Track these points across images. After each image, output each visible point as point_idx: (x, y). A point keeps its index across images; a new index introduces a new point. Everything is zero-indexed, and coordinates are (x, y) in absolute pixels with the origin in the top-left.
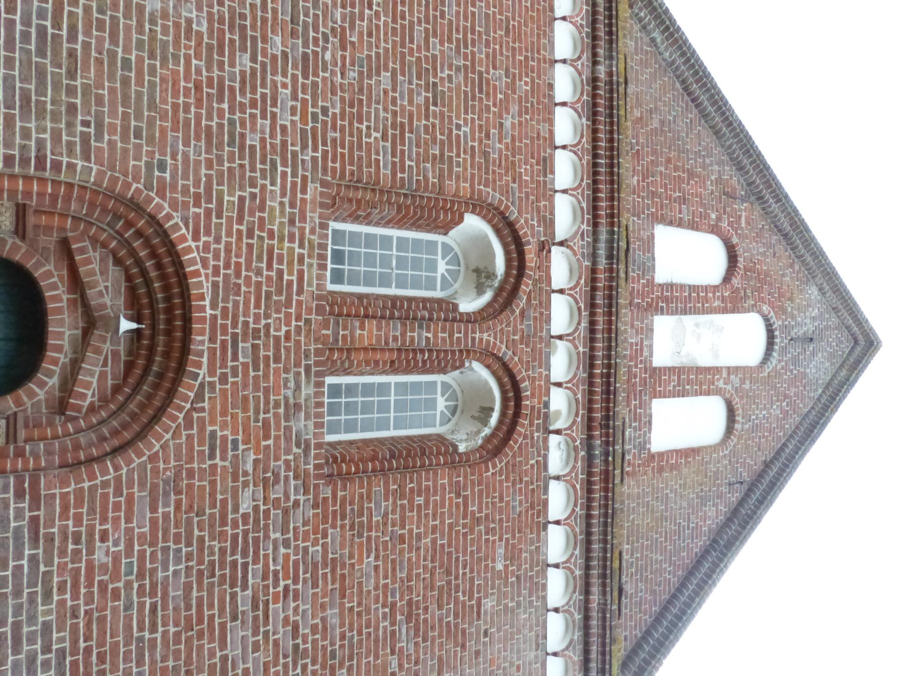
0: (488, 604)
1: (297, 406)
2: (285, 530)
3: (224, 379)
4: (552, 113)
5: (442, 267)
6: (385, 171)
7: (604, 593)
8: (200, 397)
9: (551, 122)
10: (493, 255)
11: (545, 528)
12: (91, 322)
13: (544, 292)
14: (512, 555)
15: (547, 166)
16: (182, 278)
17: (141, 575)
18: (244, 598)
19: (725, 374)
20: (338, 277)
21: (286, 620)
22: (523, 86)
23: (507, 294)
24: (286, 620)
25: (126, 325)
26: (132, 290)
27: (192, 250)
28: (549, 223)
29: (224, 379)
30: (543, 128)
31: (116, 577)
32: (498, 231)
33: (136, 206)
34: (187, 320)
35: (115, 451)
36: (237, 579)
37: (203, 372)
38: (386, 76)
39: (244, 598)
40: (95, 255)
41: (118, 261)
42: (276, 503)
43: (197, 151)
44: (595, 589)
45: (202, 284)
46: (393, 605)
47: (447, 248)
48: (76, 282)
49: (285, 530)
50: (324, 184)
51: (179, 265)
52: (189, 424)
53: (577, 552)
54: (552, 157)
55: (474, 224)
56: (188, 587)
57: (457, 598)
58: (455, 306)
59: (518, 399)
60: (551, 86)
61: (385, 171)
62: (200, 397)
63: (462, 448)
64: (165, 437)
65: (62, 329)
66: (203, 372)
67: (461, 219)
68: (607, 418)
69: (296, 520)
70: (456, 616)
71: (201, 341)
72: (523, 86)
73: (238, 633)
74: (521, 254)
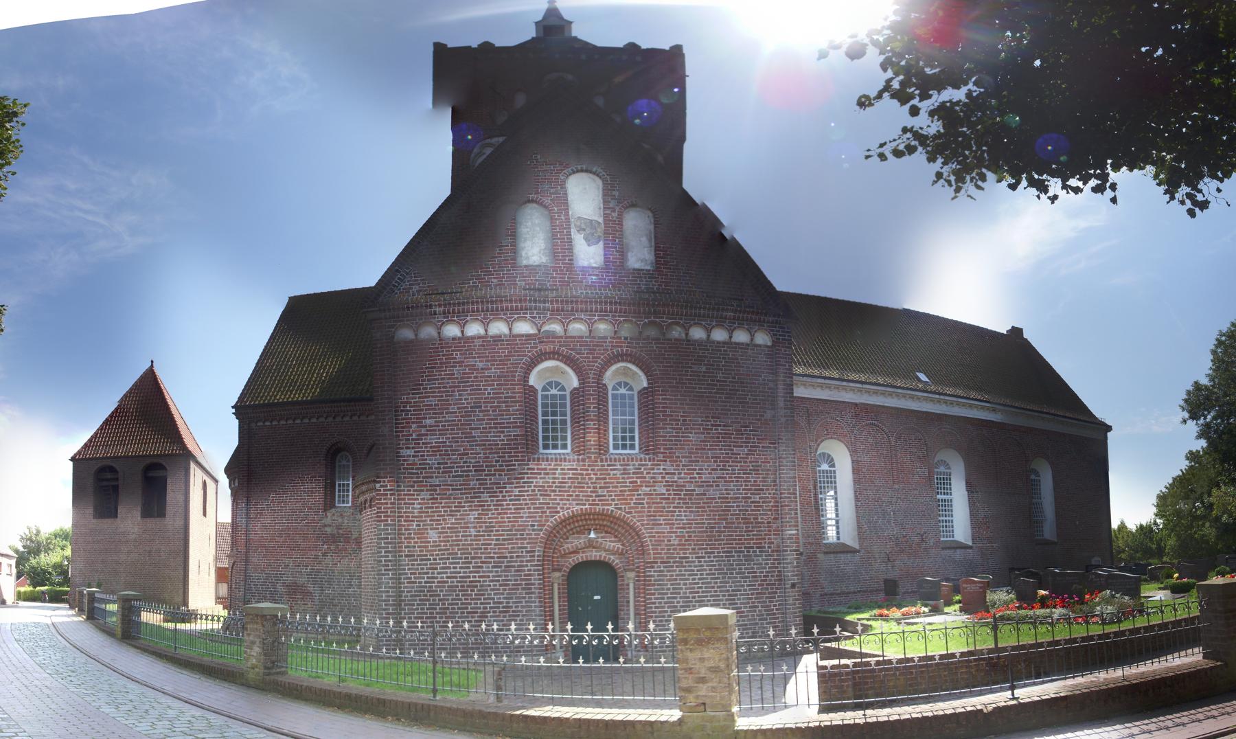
5: (554, 392)
10: (547, 369)
13: (568, 339)
20: (564, 446)
23: (569, 361)
25: (592, 535)
26: (578, 533)
28: (529, 337)
35: (639, 536)
40: (566, 546)
47: (544, 389)
48: (576, 552)
55: (532, 381)
58: (575, 389)
59: (622, 355)
63: (645, 384)
65: (594, 555)
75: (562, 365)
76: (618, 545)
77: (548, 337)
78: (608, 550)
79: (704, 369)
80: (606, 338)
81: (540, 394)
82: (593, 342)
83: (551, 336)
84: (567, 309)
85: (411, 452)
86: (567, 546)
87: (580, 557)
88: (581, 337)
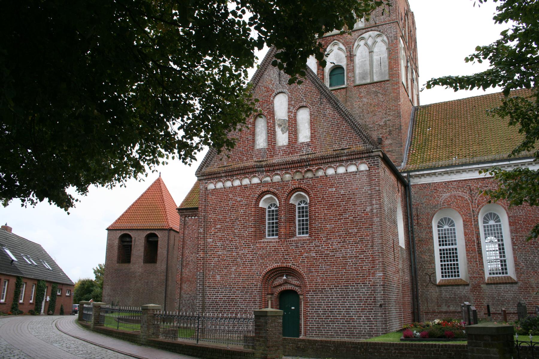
0: (342, 192)
1: (296, 245)
2: (319, 246)
3: (291, 260)
4: (235, 187)
6: (253, 230)
7: (342, 156)
8: (294, 265)
9: (237, 187)
11: (327, 176)
12: (286, 282)
14: (332, 186)
15: (246, 186)
16: (274, 269)
17: (324, 274)
18: (331, 254)
19: (290, 114)
21: (337, 245)
22: (231, 196)
24: (337, 245)
25: (285, 278)
27: (270, 267)
29: (291, 260)
30: (239, 189)
31: (324, 278)
32: (262, 198)
33: (264, 277)
34: (282, 267)
36: (327, 255)
37: (290, 264)
38: (236, 231)
39: (331, 254)
41: (276, 279)
42: (314, 248)
43: (254, 268)
44: (342, 158)
45: (275, 265)
46: (338, 219)
47: (269, 208)
48: (280, 285)
49: (319, 246)
50: (256, 243)
51: (273, 269)
52: (298, 266)
53: (332, 165)
54: (244, 186)
56: (327, 265)
57: (340, 202)
59: (297, 188)
60: (230, 188)
61: (253, 230)
62: (294, 265)
64: (301, 270)
65: (289, 287)
66: (290, 264)
67: (261, 208)
68: (299, 162)
69: (318, 244)
70: (344, 201)
71: (284, 265)
72: (231, 196)
73: (338, 254)
74: (265, 192)
75: (273, 196)
76: (298, 282)
77: (265, 184)
78: (294, 285)
79: (334, 189)
80: (289, 181)
81: (267, 210)
82: (283, 184)
83: (266, 183)
84: (272, 169)
85: (211, 240)
86: (276, 283)
87: (283, 288)
88: (278, 182)
